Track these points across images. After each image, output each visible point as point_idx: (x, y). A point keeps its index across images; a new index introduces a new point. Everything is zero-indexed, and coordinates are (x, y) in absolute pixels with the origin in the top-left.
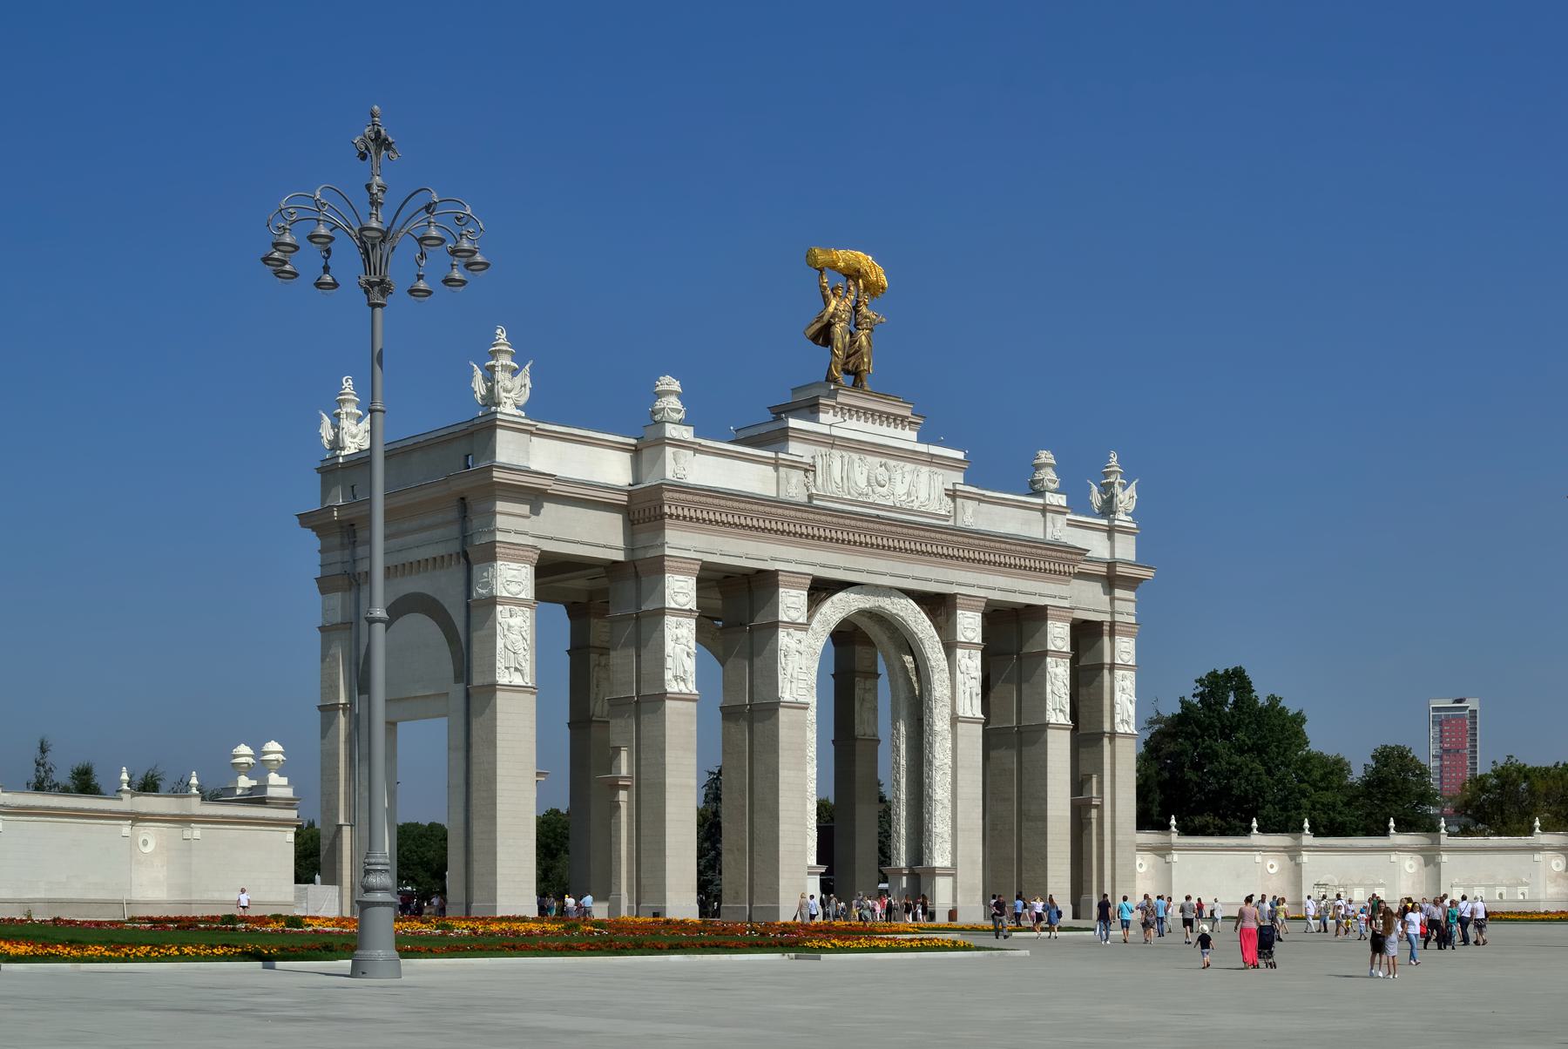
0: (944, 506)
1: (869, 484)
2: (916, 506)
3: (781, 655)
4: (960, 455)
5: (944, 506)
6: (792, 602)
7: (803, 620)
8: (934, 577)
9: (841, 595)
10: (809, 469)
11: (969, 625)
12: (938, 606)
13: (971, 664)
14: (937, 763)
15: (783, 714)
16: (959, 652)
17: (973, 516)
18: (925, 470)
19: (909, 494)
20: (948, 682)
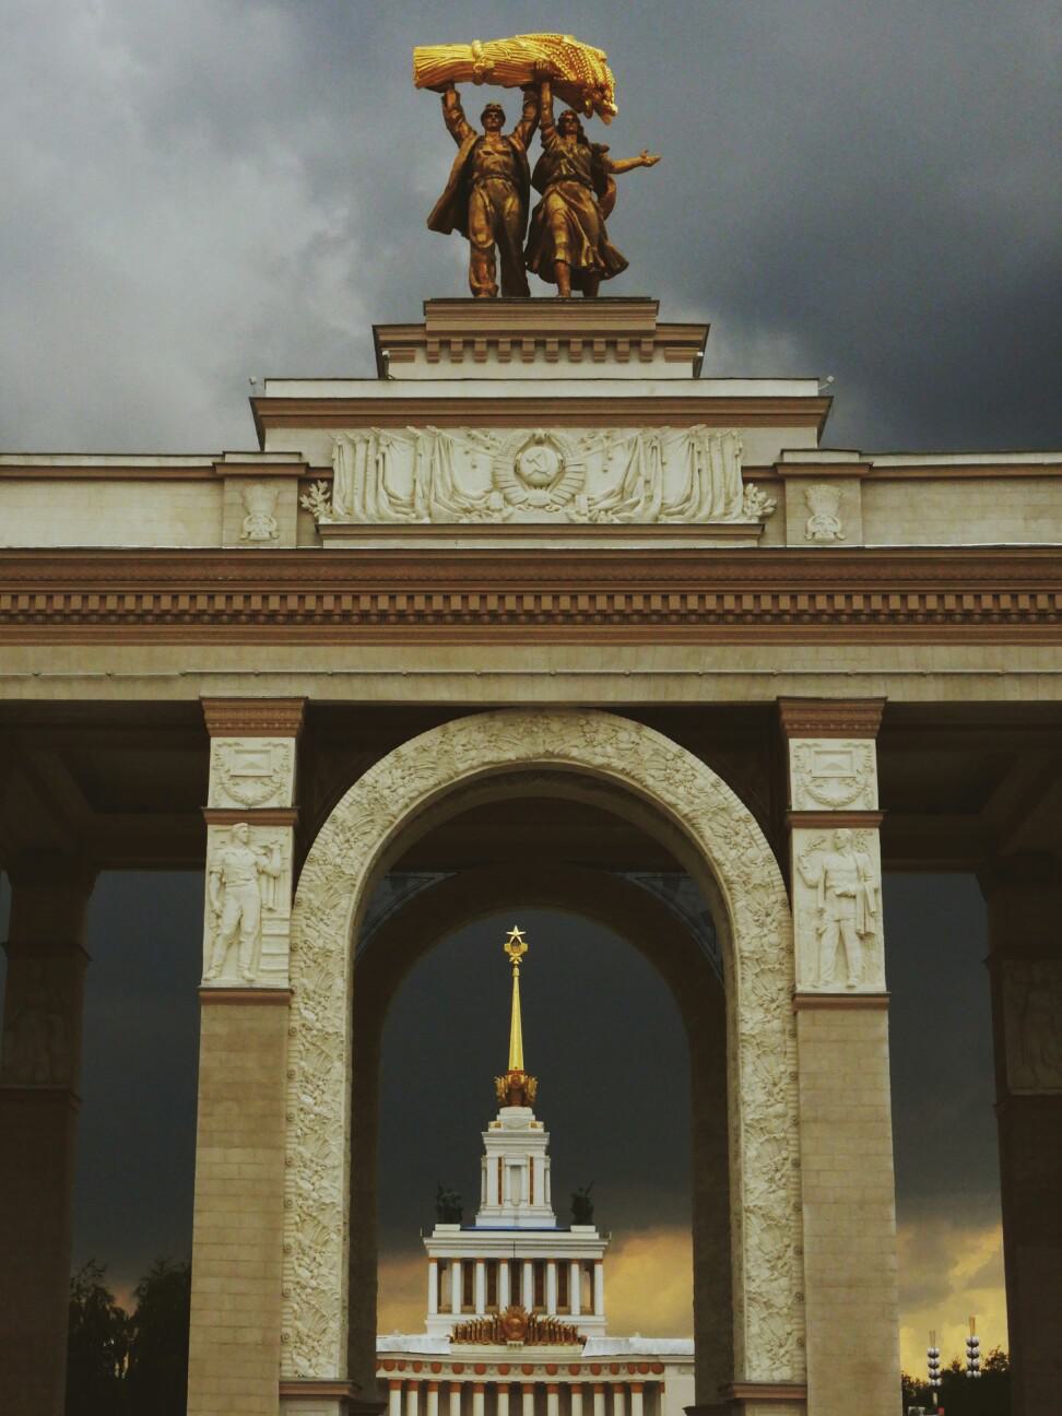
0: (748, 506)
1: (496, 485)
2: (643, 514)
3: (211, 884)
4: (810, 389)
5: (748, 506)
6: (252, 769)
7: (286, 798)
8: (716, 671)
9: (429, 738)
10: (309, 477)
11: (833, 771)
12: (747, 746)
13: (845, 869)
14: (748, 1114)
15: (212, 1023)
16: (800, 839)
17: (825, 519)
18: (676, 439)
19: (622, 492)
20: (779, 913)
